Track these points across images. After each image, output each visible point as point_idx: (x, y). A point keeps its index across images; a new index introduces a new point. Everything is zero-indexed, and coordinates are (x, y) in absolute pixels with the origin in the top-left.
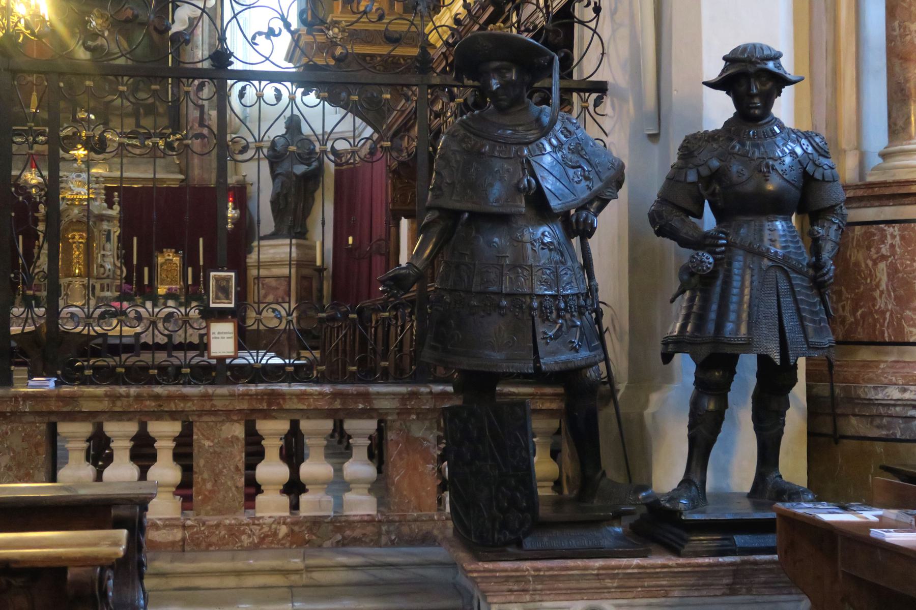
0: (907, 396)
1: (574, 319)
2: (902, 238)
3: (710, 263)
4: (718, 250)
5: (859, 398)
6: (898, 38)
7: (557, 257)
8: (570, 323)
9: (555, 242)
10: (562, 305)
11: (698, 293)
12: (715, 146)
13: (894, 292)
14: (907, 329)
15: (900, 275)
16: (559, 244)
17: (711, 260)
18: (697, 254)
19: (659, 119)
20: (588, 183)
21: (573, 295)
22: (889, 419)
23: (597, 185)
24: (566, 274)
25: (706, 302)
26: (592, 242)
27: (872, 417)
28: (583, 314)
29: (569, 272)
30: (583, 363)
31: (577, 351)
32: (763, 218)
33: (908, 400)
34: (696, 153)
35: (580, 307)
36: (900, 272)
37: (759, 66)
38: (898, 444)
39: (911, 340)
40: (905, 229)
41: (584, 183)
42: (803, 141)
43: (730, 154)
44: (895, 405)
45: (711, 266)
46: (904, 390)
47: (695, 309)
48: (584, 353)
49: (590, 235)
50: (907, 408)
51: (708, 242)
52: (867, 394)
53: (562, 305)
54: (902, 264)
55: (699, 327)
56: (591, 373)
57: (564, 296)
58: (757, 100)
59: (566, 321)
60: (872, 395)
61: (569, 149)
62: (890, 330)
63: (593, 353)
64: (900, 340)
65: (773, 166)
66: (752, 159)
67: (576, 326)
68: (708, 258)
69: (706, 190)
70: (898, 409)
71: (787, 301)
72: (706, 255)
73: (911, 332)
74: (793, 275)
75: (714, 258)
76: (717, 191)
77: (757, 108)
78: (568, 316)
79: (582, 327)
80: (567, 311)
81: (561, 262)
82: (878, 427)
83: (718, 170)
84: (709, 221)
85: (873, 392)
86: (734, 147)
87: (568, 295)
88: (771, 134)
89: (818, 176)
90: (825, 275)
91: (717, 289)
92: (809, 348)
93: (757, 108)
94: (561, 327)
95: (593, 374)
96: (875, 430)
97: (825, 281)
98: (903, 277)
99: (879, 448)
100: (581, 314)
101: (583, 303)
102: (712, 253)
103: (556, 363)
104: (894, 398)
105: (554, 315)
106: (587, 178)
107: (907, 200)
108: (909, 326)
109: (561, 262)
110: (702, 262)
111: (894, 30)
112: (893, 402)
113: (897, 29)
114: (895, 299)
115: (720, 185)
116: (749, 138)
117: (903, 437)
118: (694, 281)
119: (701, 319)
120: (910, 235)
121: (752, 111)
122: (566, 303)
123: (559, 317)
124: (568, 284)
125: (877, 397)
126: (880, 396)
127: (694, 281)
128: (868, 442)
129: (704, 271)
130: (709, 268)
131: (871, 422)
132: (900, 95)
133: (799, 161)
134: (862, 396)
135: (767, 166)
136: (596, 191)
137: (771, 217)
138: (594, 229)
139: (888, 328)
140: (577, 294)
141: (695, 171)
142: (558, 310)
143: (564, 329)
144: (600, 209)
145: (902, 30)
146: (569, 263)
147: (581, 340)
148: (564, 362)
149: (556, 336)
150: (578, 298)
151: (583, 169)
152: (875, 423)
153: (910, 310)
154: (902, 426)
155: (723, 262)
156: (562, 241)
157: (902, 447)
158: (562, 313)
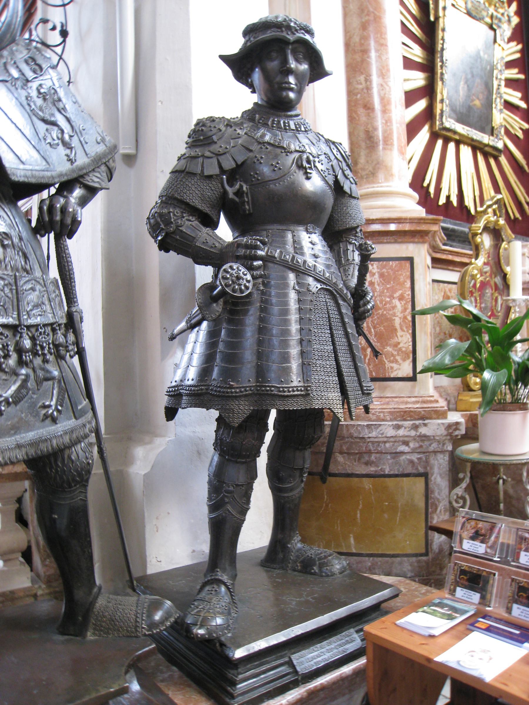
0: (401, 432)
1: (49, 367)
2: (381, 275)
3: (248, 281)
4: (255, 263)
5: (351, 436)
6: (365, 91)
7: (20, 261)
8: (41, 374)
9: (13, 233)
10: (27, 343)
11: (225, 325)
12: (239, 131)
13: (374, 328)
14: (388, 365)
15: (380, 312)
16: (21, 239)
17: (249, 277)
18: (231, 267)
19: (137, 141)
20: (68, 151)
21: (45, 325)
22: (378, 455)
23: (82, 160)
24: (33, 289)
25: (236, 334)
26: (72, 245)
27: (361, 454)
28: (63, 358)
29: (38, 287)
30: (67, 439)
31: (54, 420)
32: (301, 228)
33: (402, 436)
34: (215, 138)
35: (57, 346)
36: (380, 309)
37: (298, 35)
38: (387, 479)
39: (392, 376)
40: (384, 267)
41: (62, 150)
42: (332, 146)
43: (260, 143)
44: (385, 442)
45: (250, 285)
46: (398, 427)
47: (221, 347)
48: (67, 424)
49: (70, 235)
50: (396, 444)
51: (242, 252)
52: (360, 433)
53: (27, 343)
54: (381, 302)
55: (229, 374)
56: (78, 452)
57: (29, 327)
58: (292, 79)
59: (34, 370)
60: (366, 433)
61: (39, 93)
62: (371, 367)
63: (80, 421)
64: (381, 376)
65: (314, 162)
66: (288, 152)
67: (53, 378)
68: (245, 275)
69: (231, 186)
70: (387, 445)
71: (339, 333)
72: (243, 269)
73: (392, 368)
74: (341, 302)
75: (252, 276)
76: (245, 189)
77: (292, 90)
78: (38, 361)
79: (62, 379)
80: (35, 354)
81: (25, 270)
82: (367, 464)
83: (243, 163)
84: (224, 232)
85: (366, 431)
86: (263, 135)
87: (36, 326)
88: (303, 129)
89: (346, 188)
90: (369, 302)
91: (251, 321)
92: (363, 394)
93: (292, 90)
94: (25, 381)
95: (81, 453)
96: (363, 466)
97: (368, 311)
98: (383, 315)
99: (367, 484)
100: (59, 357)
101: (61, 339)
102: (250, 268)
103: (19, 446)
104: (389, 435)
105: (12, 362)
106: (67, 145)
107: (382, 239)
108: (390, 362)
109: (25, 270)
110: (238, 278)
111: (361, 84)
112: (385, 439)
113: (363, 82)
114: (375, 336)
115: (246, 182)
116: (279, 127)
117: (392, 473)
118: (218, 307)
119: (232, 358)
120: (388, 272)
121: (284, 94)
122: (33, 339)
123: (21, 363)
124: (36, 306)
125: (370, 435)
126: (374, 434)
127: (218, 307)
128: (356, 479)
129: (242, 291)
130: (247, 288)
131: (359, 459)
132: (368, 142)
133: (332, 166)
134: (355, 435)
135: (308, 162)
136: (81, 169)
137: (310, 227)
138: (75, 224)
139: (369, 364)
140: (52, 324)
141: (215, 161)
142: (20, 351)
143: (31, 384)
144: (83, 202)
145: (368, 83)
146: (38, 273)
147: (60, 401)
148: (34, 444)
149: (17, 398)
150: (54, 330)
151: (62, 132)
152: (363, 460)
153: (390, 345)
154: (390, 461)
155: (263, 281)
156: (24, 235)
157: (390, 482)
158: (28, 357)
